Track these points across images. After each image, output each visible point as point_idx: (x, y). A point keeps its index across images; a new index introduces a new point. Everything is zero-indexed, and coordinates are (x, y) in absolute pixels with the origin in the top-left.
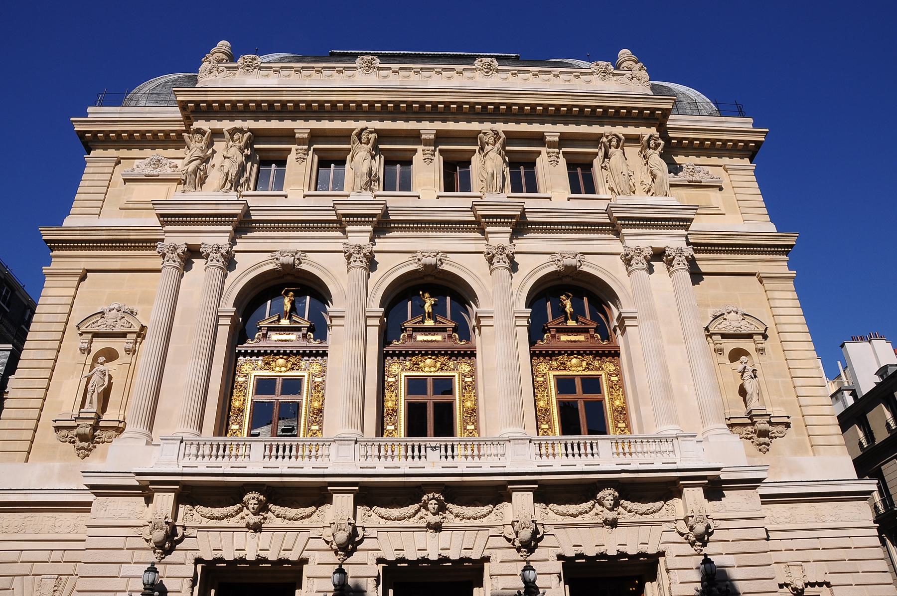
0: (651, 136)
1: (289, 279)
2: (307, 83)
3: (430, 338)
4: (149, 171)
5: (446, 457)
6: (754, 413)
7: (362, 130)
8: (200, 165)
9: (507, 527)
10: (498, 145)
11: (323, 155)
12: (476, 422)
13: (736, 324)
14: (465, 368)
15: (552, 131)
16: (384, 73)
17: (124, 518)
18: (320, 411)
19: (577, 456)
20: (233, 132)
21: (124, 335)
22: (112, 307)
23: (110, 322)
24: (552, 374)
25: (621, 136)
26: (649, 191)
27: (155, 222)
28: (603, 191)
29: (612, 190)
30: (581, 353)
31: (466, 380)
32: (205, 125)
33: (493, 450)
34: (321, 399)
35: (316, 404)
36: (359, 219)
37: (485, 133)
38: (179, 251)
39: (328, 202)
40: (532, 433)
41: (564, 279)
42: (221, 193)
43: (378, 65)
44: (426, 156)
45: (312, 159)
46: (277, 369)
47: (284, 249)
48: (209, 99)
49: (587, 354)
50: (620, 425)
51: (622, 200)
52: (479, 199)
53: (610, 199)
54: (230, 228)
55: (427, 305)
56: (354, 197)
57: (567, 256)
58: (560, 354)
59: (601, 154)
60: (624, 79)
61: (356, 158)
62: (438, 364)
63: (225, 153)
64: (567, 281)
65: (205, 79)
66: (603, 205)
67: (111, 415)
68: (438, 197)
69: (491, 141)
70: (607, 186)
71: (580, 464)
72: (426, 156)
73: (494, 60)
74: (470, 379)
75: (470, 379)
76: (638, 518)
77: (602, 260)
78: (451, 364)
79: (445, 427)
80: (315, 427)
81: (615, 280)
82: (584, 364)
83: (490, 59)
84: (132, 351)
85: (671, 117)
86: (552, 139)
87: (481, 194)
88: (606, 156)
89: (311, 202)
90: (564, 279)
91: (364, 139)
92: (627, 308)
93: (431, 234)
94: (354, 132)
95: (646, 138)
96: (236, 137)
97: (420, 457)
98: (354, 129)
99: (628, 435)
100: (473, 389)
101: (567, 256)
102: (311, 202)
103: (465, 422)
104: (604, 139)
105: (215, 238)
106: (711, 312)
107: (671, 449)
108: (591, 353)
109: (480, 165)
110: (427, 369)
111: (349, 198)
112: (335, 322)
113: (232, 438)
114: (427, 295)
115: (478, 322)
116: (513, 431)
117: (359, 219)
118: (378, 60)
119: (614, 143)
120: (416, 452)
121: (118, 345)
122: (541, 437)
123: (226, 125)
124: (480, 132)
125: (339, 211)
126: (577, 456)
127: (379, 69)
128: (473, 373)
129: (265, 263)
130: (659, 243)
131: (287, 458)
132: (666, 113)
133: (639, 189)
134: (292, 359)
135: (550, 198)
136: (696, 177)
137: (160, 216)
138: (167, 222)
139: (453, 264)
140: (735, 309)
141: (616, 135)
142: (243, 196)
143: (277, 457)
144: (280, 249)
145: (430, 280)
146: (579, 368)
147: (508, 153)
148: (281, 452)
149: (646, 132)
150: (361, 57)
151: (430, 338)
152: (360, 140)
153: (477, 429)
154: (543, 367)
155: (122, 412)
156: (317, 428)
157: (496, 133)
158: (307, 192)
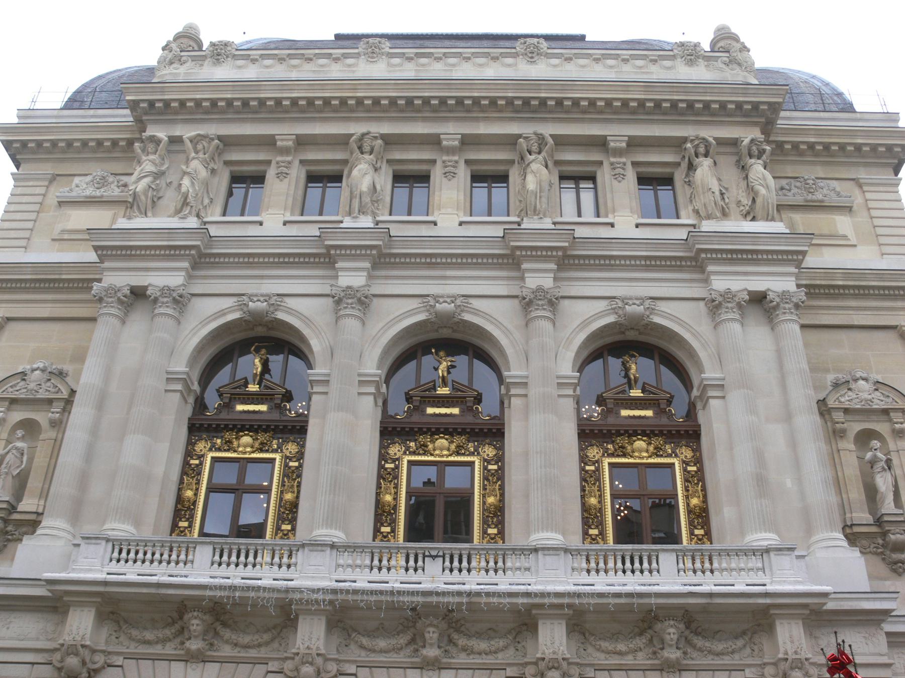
0: (752, 141)
1: (260, 331)
2: (294, 75)
3: (443, 411)
4: (90, 191)
5: (451, 570)
6: (886, 518)
7: (363, 135)
8: (152, 182)
9: (529, 667)
10: (544, 154)
11: (312, 168)
12: (501, 524)
13: (865, 396)
14: (489, 451)
15: (618, 132)
16: (396, 61)
18: (294, 507)
19: (629, 573)
20: (194, 140)
21: (50, 401)
22: (35, 366)
23: (32, 386)
24: (606, 461)
25: (711, 139)
26: (748, 213)
27: (92, 257)
29: (697, 212)
30: (647, 432)
31: (490, 467)
32: (161, 133)
33: (521, 562)
35: (289, 496)
36: (354, 252)
37: (526, 138)
38: (119, 295)
39: (314, 231)
40: (575, 541)
41: (627, 333)
42: (176, 219)
43: (387, 50)
44: (447, 169)
45: (297, 173)
46: (240, 449)
47: (255, 292)
48: (166, 97)
49: (656, 435)
50: (697, 532)
51: (707, 226)
52: (516, 226)
53: (694, 226)
54: (186, 264)
55: (441, 367)
56: (348, 223)
58: (618, 433)
59: (684, 165)
61: (355, 172)
62: (453, 447)
63: (184, 167)
64: (631, 335)
65: (164, 72)
66: (682, 234)
67: (28, 504)
68: (461, 224)
69: (535, 148)
70: (690, 208)
71: (632, 583)
72: (447, 169)
73: (542, 40)
74: (495, 467)
75: (495, 467)
76: (615, 661)
77: (677, 309)
78: (471, 447)
79: (458, 529)
80: (286, 527)
81: (695, 335)
82: (651, 448)
83: (536, 40)
84: (58, 425)
85: (783, 114)
86: (285, 143)
87: (518, 220)
88: (691, 167)
89: (293, 231)
90: (627, 333)
91: (367, 148)
92: (711, 373)
93: (449, 273)
94: (354, 137)
95: (746, 141)
96: (200, 147)
97: (416, 570)
98: (352, 135)
99: (500, 544)
100: (498, 479)
101: (441, 300)
102: (293, 231)
103: (485, 523)
104: (689, 145)
105: (164, 278)
106: (830, 377)
107: (760, 565)
108: (661, 434)
109: (519, 180)
110: (437, 452)
111: (342, 225)
112: (316, 389)
113: (180, 539)
114: (442, 354)
115: (508, 390)
116: (554, 538)
117: (354, 252)
118: (388, 44)
119: (702, 150)
120: (414, 562)
121: (42, 417)
122: (588, 546)
123: (187, 132)
124: (520, 136)
125: (327, 243)
126: (629, 573)
127: (391, 56)
128: (499, 459)
129: (230, 310)
130: (758, 284)
131: (241, 566)
132: (775, 108)
134: (262, 437)
135: (612, 225)
136: (819, 196)
137: (96, 248)
138: (106, 255)
139: (476, 312)
140: (864, 375)
141: (704, 139)
142: (205, 223)
143: (237, 565)
144: (250, 292)
145: (446, 333)
147: (557, 163)
148: (242, 558)
149: (748, 135)
150: (366, 40)
151: (443, 411)
152: (360, 148)
153: (501, 533)
154: (594, 452)
155: (42, 502)
156: (289, 527)
157: (541, 139)
158: (287, 219)
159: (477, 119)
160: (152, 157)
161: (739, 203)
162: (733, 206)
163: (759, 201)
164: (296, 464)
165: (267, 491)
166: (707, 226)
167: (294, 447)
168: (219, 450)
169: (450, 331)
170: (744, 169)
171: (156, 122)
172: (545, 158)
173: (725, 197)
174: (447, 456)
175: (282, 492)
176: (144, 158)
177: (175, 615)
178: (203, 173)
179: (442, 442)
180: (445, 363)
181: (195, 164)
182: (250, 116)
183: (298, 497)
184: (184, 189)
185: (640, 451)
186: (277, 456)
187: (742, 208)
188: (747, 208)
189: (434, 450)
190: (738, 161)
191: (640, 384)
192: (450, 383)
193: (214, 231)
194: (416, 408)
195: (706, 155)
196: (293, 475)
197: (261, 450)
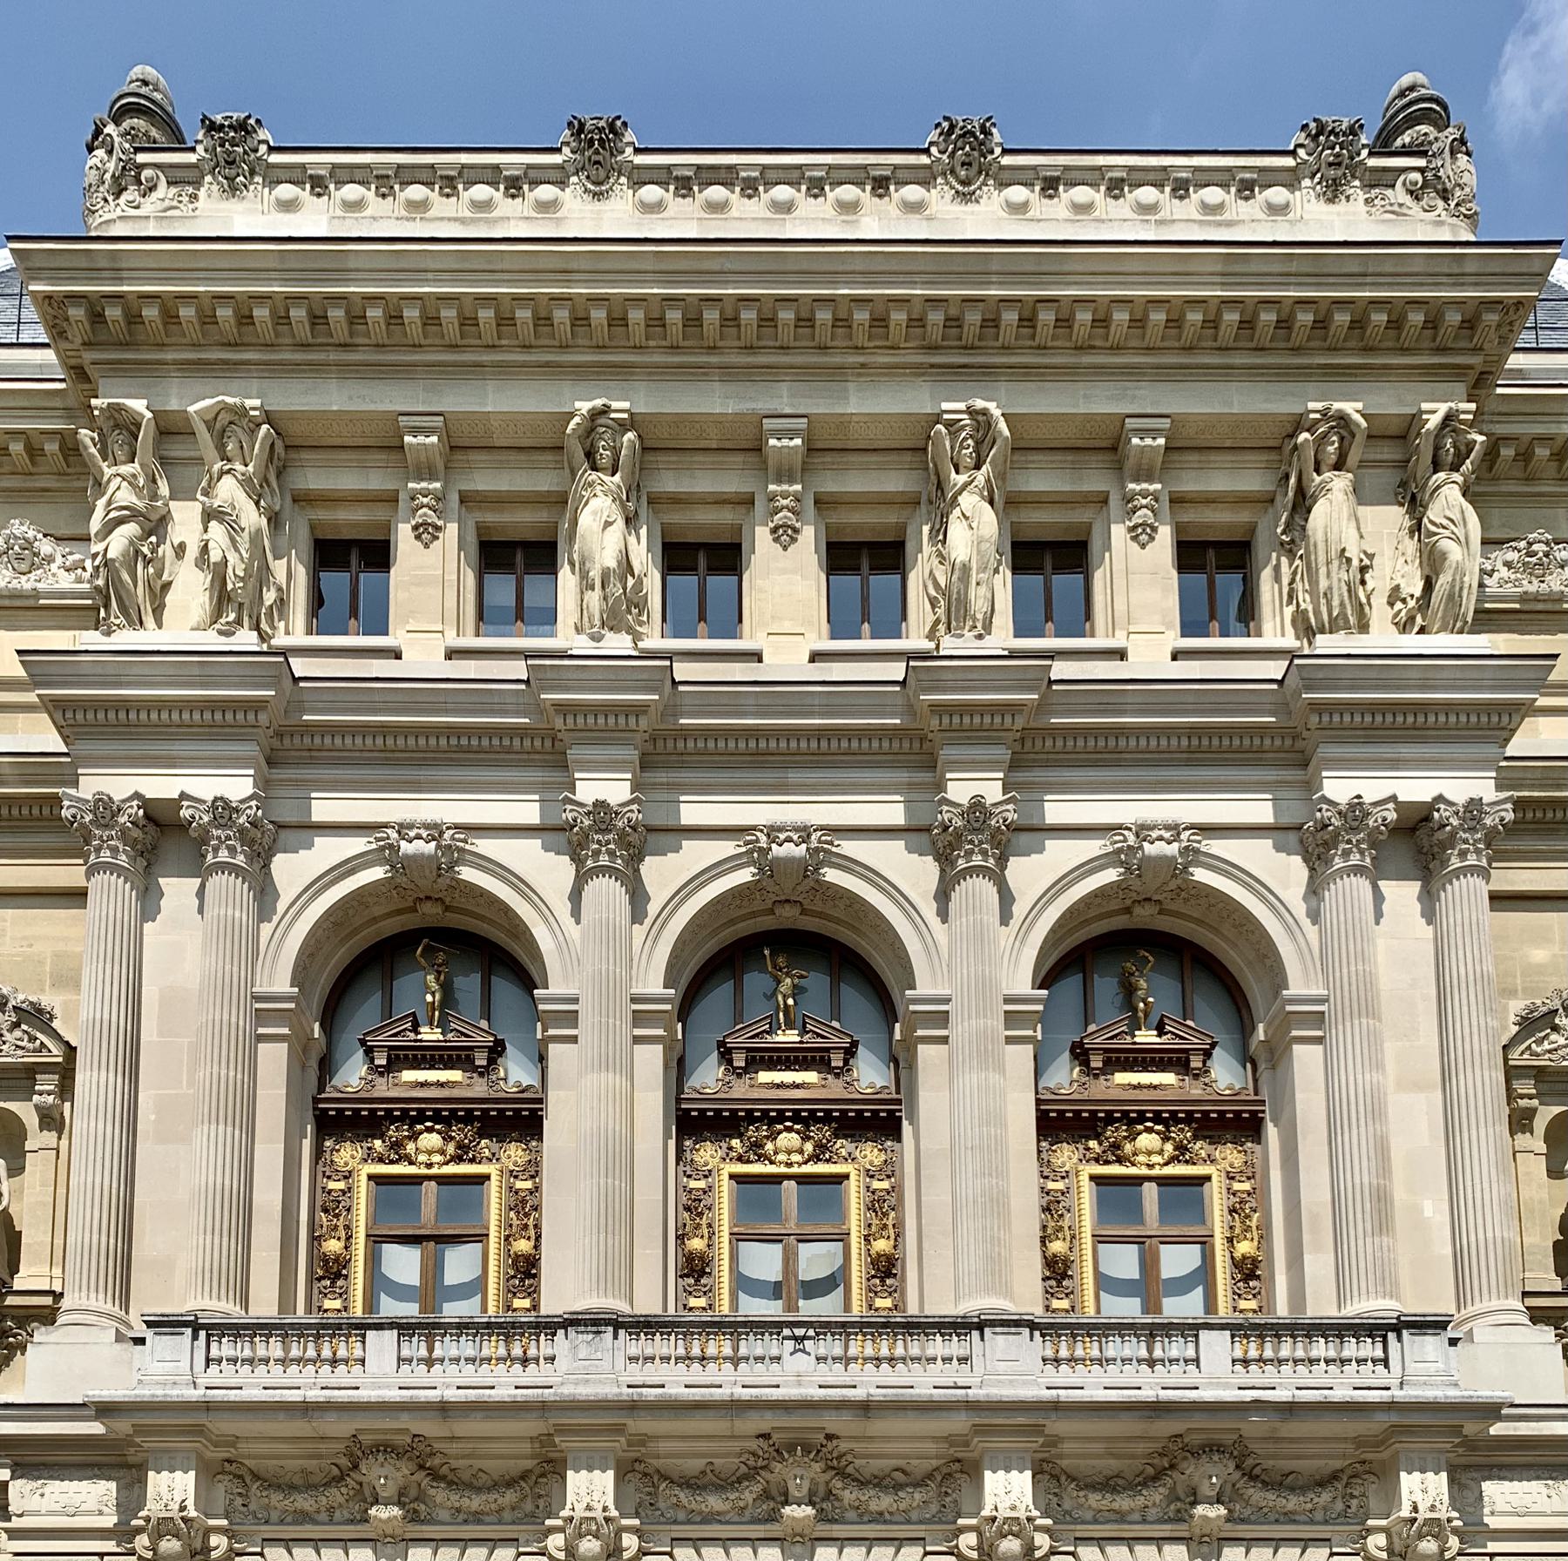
17: (89, 1513)
28: (1276, 631)
34: (532, 1232)
41: (1138, 910)
57: (1155, 834)
60: (1399, 194)
64: (1145, 917)
88: (1303, 503)
90: (1138, 910)
91: (604, 456)
133: (1380, 614)
146: (1156, 1159)
159: (837, 374)
160: (126, 469)
161: (1395, 596)
162: (1380, 601)
163: (1443, 583)
164: (529, 1185)
165: (482, 1238)
166: (1325, 643)
167: (520, 1153)
168: (381, 1160)
169: (796, 911)
170: (1415, 504)
171: (119, 369)
172: (988, 481)
173: (1367, 577)
174: (800, 1165)
175: (507, 1238)
176: (108, 471)
177: (344, 1462)
178: (251, 517)
179: (788, 1139)
180: (788, 980)
181: (229, 491)
182: (333, 356)
183: (536, 1247)
184: (215, 556)
185: (1149, 1153)
186: (490, 1169)
187: (1399, 605)
188: (1412, 603)
189: (776, 1153)
190: (1403, 484)
191: (1155, 1020)
192: (799, 1023)
193: (300, 666)
194: (739, 1073)
195: (1338, 466)
196: (525, 1207)
197: (458, 1159)
